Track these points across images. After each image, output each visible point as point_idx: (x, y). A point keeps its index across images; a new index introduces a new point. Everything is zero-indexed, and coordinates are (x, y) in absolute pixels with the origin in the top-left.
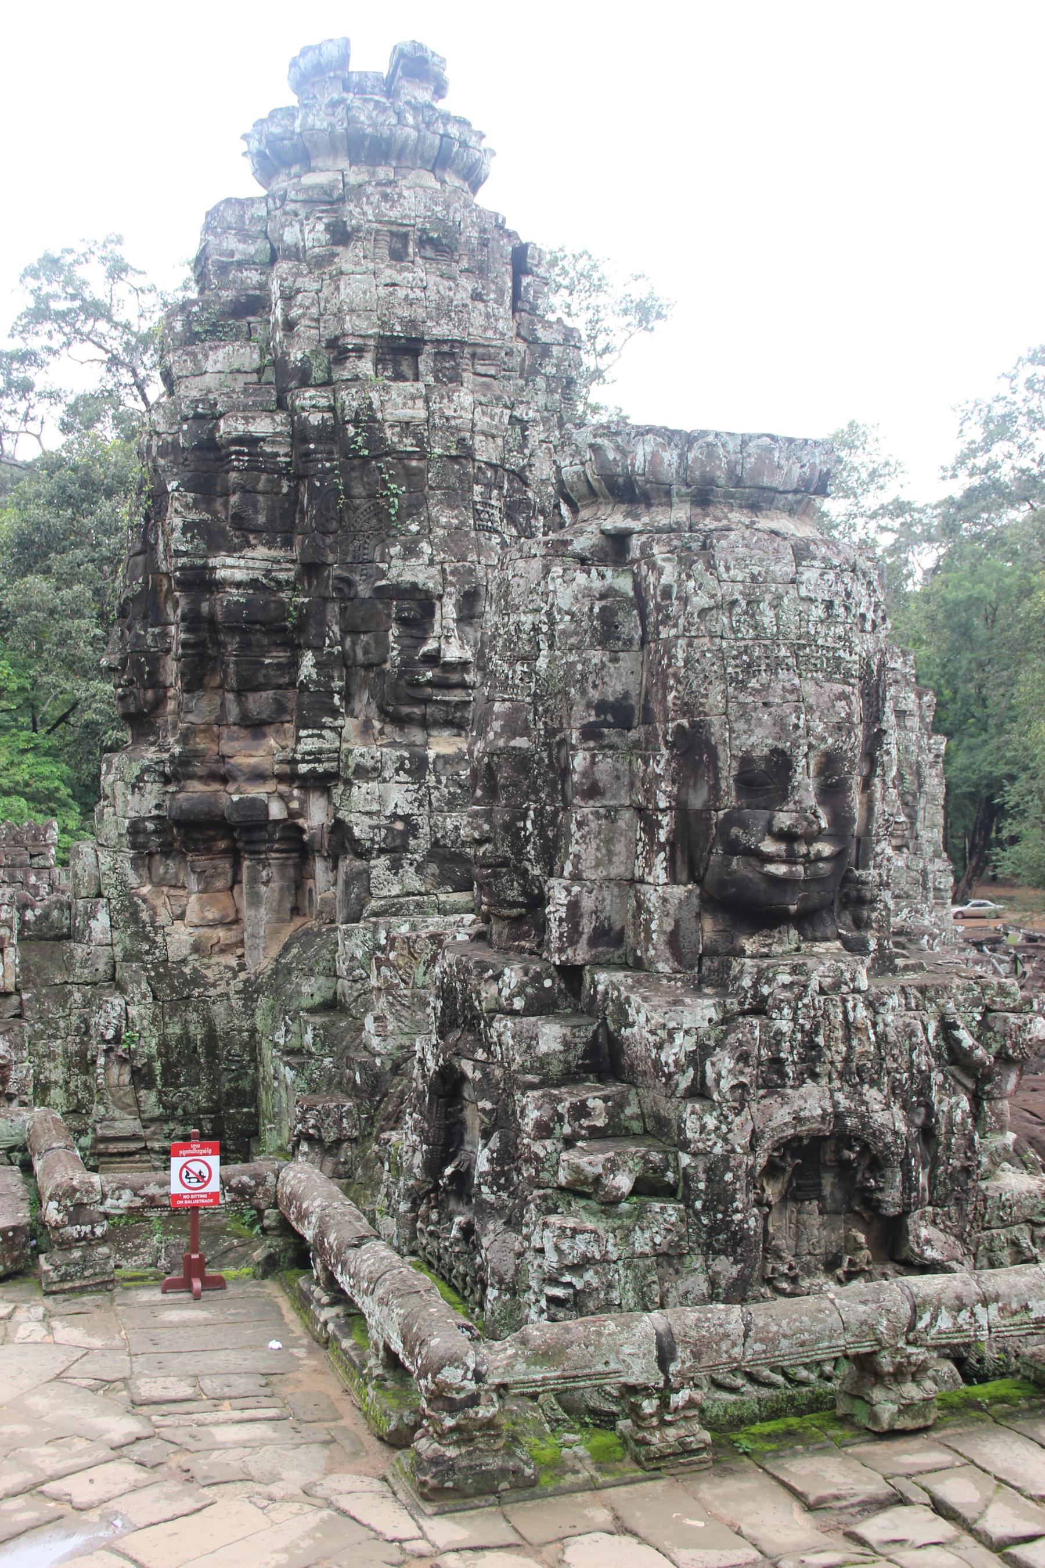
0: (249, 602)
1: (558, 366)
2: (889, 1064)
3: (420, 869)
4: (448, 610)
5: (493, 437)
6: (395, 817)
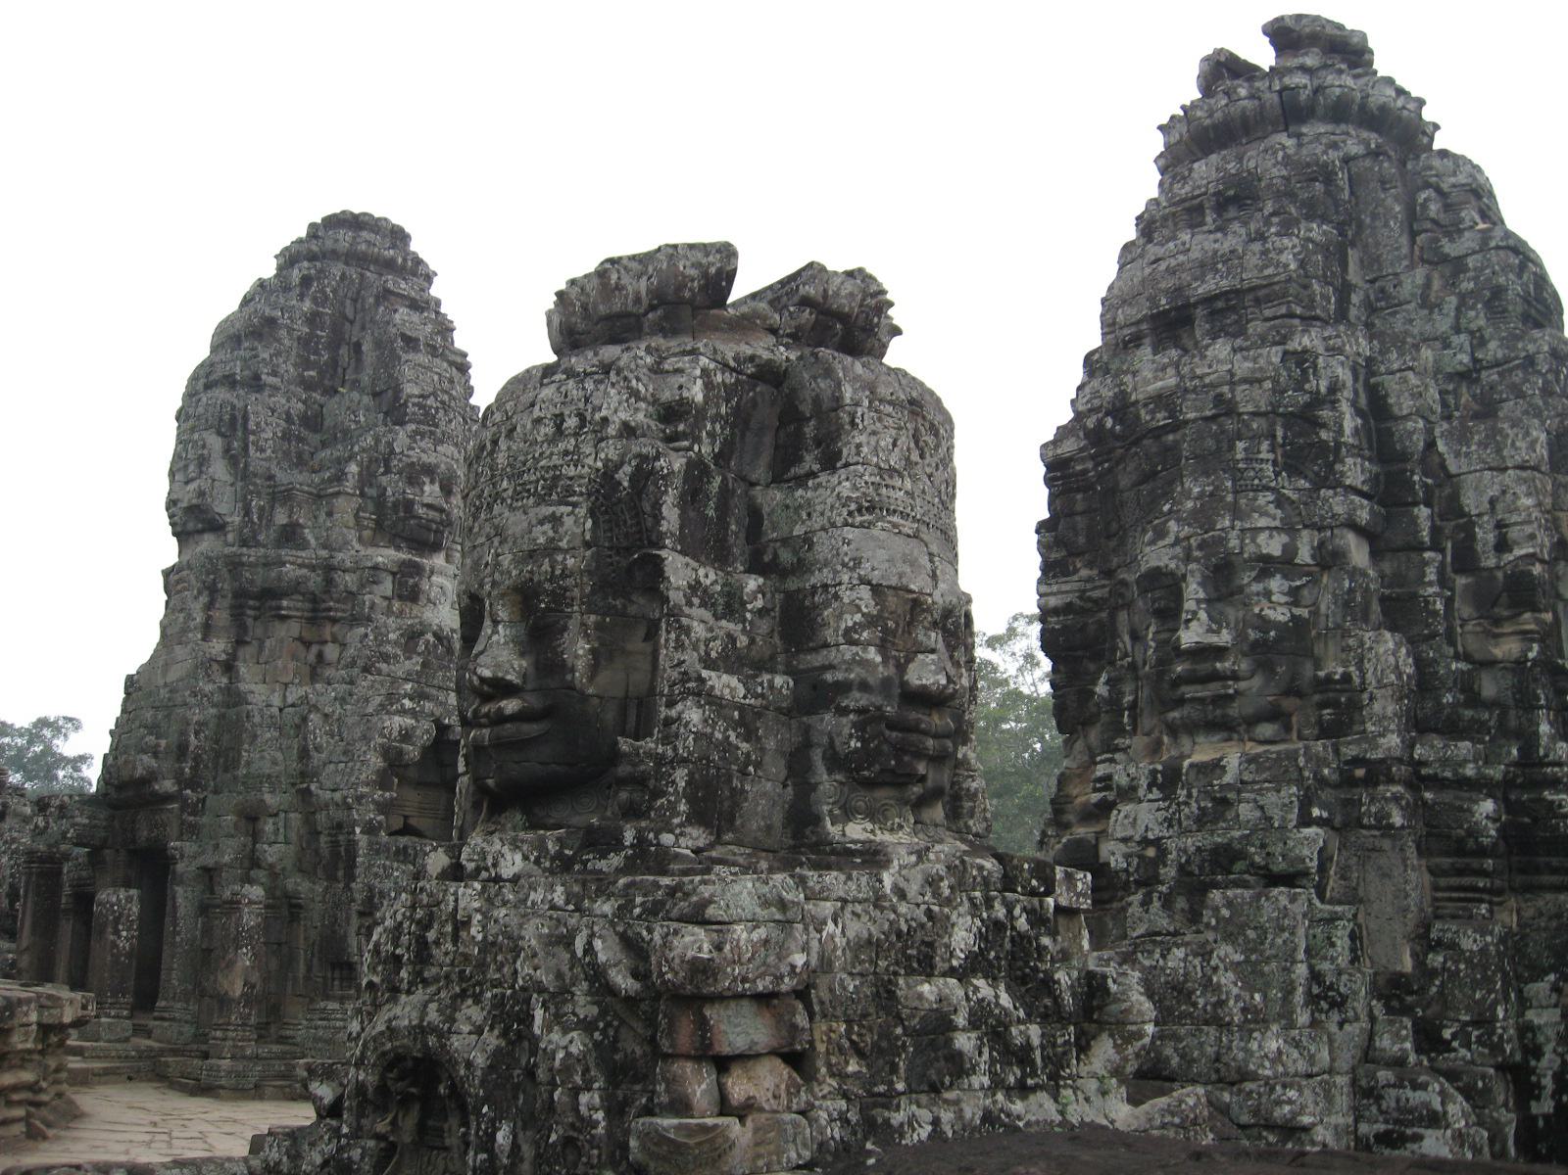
0: (1065, 627)
1: (1476, 279)
2: (493, 975)
3: (1167, 903)
4: (1193, 591)
5: (1260, 381)
6: (1145, 842)
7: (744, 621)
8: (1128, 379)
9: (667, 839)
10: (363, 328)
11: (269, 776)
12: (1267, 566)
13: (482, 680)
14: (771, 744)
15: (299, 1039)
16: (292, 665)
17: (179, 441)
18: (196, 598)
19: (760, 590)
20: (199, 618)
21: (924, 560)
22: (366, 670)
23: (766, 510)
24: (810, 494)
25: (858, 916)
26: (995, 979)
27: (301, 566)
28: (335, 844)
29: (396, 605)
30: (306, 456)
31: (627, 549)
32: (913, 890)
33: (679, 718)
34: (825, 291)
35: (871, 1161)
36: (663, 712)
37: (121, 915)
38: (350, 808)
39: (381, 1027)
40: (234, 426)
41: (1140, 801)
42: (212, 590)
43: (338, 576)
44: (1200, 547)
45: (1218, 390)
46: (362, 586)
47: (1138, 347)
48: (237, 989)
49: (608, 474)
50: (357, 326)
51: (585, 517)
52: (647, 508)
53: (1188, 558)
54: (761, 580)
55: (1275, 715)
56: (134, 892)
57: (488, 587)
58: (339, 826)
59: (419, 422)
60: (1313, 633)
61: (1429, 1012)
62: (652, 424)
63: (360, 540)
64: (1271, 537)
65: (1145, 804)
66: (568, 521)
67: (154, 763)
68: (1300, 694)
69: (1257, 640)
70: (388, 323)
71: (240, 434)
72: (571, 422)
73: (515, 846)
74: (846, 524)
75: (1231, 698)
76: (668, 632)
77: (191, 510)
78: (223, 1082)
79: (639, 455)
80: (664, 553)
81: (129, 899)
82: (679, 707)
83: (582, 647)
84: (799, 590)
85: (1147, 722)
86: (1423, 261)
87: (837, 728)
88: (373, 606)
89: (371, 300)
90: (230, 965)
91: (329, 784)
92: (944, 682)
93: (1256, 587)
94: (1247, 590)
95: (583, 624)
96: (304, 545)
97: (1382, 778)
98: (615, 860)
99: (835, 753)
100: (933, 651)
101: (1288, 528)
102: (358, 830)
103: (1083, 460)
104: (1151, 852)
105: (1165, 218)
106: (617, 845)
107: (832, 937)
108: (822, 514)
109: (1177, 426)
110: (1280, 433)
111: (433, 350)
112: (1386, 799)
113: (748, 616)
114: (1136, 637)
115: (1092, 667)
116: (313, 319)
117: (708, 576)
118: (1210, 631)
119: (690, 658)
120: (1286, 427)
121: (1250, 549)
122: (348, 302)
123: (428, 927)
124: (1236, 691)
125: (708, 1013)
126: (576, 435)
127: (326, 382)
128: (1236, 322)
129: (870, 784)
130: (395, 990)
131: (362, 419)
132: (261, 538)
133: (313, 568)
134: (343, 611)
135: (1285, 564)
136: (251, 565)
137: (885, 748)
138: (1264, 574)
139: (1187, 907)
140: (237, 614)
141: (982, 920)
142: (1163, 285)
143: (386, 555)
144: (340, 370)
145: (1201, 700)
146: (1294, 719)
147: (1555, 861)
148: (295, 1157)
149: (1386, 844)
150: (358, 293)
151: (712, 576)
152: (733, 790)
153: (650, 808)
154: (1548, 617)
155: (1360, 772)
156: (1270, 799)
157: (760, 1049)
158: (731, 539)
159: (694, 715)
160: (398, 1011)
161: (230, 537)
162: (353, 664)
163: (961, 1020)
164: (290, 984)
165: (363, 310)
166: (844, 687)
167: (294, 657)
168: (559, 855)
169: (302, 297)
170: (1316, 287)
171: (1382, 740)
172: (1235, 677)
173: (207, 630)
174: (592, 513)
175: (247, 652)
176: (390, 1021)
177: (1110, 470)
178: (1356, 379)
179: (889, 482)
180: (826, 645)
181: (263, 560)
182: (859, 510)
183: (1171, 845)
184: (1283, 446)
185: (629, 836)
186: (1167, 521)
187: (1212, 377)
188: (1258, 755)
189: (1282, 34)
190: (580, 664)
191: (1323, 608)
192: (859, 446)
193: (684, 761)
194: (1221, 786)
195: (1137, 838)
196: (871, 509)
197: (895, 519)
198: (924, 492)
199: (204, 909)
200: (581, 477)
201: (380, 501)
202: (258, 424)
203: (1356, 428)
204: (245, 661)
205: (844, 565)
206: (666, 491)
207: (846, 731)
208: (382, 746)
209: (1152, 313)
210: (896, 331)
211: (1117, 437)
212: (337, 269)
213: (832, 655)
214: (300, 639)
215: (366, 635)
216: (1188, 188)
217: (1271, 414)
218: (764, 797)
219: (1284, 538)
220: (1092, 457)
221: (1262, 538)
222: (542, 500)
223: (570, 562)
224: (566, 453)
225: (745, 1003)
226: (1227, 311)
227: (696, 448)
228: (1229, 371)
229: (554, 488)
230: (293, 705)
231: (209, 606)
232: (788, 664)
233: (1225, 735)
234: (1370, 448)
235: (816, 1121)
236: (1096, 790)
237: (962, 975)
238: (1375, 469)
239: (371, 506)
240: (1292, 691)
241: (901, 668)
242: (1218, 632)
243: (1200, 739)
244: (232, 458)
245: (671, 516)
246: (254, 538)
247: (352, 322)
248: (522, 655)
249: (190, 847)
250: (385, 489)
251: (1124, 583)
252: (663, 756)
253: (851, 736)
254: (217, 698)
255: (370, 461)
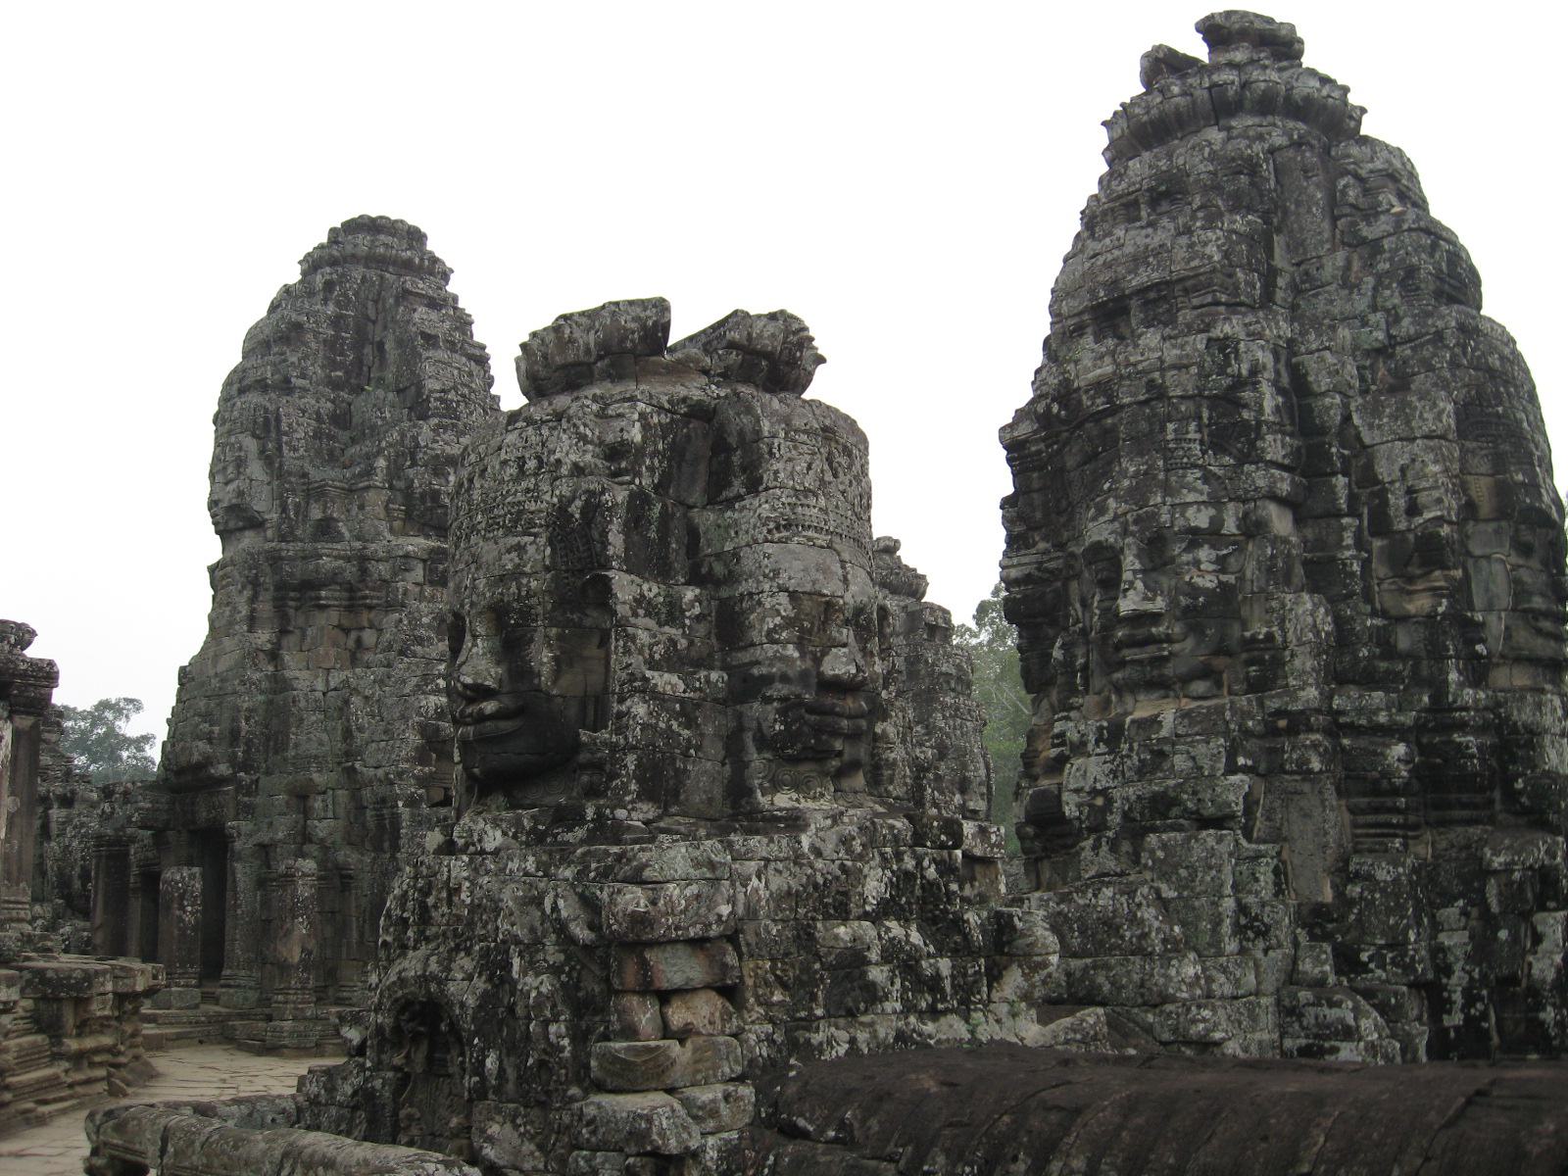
0: (1025, 597)
1: (1391, 259)
3: (1114, 847)
4: (1130, 562)
5: (1187, 367)
6: (1094, 792)
7: (683, 626)
8: (1070, 367)
9: (621, 813)
10: (385, 328)
11: (316, 757)
12: (1195, 537)
13: (466, 686)
14: (709, 730)
15: (355, 1000)
16: (333, 652)
17: (217, 444)
18: (240, 592)
19: (697, 599)
20: (244, 611)
21: (837, 568)
22: (402, 653)
23: (702, 529)
24: (736, 515)
25: (780, 872)
26: (907, 920)
27: (337, 558)
28: (380, 817)
29: (428, 590)
30: (337, 453)
31: (581, 571)
32: (828, 849)
33: (628, 712)
34: (749, 334)
35: (793, 1074)
36: (616, 707)
37: (185, 891)
38: (392, 783)
39: (393, 978)
40: (266, 428)
41: (1089, 756)
42: (255, 584)
43: (371, 566)
44: (1136, 522)
45: (1150, 376)
46: (395, 574)
47: (1081, 336)
48: (296, 956)
49: (562, 508)
50: (379, 328)
51: (545, 546)
52: (596, 536)
53: (1125, 533)
54: (697, 591)
55: (1206, 673)
56: (196, 870)
57: (467, 607)
58: (383, 800)
59: (443, 416)
60: (1240, 597)
61: (1348, 937)
62: (599, 462)
63: (391, 530)
64: (1199, 510)
65: (1093, 758)
66: (531, 549)
67: (208, 748)
68: (1229, 654)
69: (1188, 606)
70: (408, 322)
71: (273, 435)
72: (531, 464)
73: (496, 824)
74: (766, 541)
75: (1166, 659)
76: (617, 640)
77: (232, 509)
78: (286, 1042)
79: (587, 491)
80: (611, 574)
81: (192, 877)
82: (628, 703)
83: (546, 656)
84: (730, 598)
85: (1097, 682)
86: (1343, 243)
87: (764, 714)
88: (405, 593)
89: (391, 301)
90: (288, 933)
91: (371, 762)
92: (854, 671)
93: (1186, 558)
94: (1178, 561)
95: (546, 636)
96: (339, 538)
97: (1302, 728)
98: (581, 832)
99: (763, 735)
100: (845, 645)
101: (1215, 502)
102: (400, 804)
103: (1036, 441)
104: (1099, 801)
105: (1104, 213)
106: (580, 820)
107: (756, 890)
108: (747, 532)
109: (1114, 410)
110: (1205, 414)
111: (452, 346)
112: (1305, 746)
113: (687, 622)
114: (1085, 604)
115: (1051, 632)
116: (337, 322)
117: (652, 590)
118: (1146, 598)
119: (636, 661)
120: (1211, 409)
121: (1180, 523)
122: (370, 303)
123: (428, 894)
124: (1170, 653)
125: (648, 956)
126: (536, 475)
127: (353, 381)
128: (1168, 311)
129: (794, 760)
130: (404, 947)
131: (388, 415)
132: (298, 532)
133: (348, 559)
134: (378, 598)
135: (1212, 535)
136: (292, 559)
137: (806, 729)
138: (1193, 545)
139: (1131, 850)
140: (280, 605)
141: (893, 872)
142: (1101, 279)
143: (416, 544)
144: (365, 369)
145: (1140, 662)
146: (1225, 676)
147: (1465, 797)
148: (331, 1090)
149: (1306, 787)
150: (379, 294)
151: (655, 590)
152: (677, 770)
153: (608, 788)
154: (1458, 573)
155: (1282, 723)
156: (1201, 750)
157: (695, 984)
158: (672, 556)
159: (640, 709)
160: (406, 964)
161: (269, 533)
162: (389, 648)
163: (874, 955)
164: (344, 949)
165: (384, 310)
166: (768, 680)
167: (335, 644)
168: (534, 830)
169: (325, 301)
170: (1240, 275)
171: (1302, 693)
172: (1169, 639)
173: (252, 621)
174: (550, 542)
175: (291, 640)
176: (400, 972)
177: (1060, 450)
178: (1277, 359)
179: (804, 501)
180: (753, 645)
181: (300, 554)
182: (777, 528)
183: (1116, 794)
184: (1209, 426)
185: (590, 813)
186: (1106, 499)
187: (1145, 364)
188: (1192, 710)
189: (1214, 30)
190: (545, 670)
191: (1248, 574)
192: (776, 472)
193: (634, 748)
194: (1158, 739)
195: (1087, 789)
196: (787, 527)
197: (810, 533)
198: (837, 507)
199: (261, 883)
200: (541, 511)
201: (408, 493)
202: (290, 425)
203: (1277, 406)
204: (289, 649)
205: (765, 576)
206: (611, 521)
207: (771, 717)
208: (420, 724)
209: (1095, 305)
210: (821, 360)
211: (1063, 422)
212: (357, 273)
213: (757, 653)
214: (339, 626)
215: (401, 621)
216: (1124, 185)
217: (1197, 397)
218: (704, 774)
219: (1212, 512)
220: (1043, 440)
221: (1190, 512)
222: (509, 531)
223: (534, 584)
224: (528, 490)
225: (679, 946)
226: (1159, 301)
227: (637, 481)
228: (1159, 358)
229: (520, 521)
230: (335, 689)
231: (253, 599)
232: (724, 661)
233: (1162, 692)
234: (1292, 424)
235: (747, 1041)
236: (1054, 746)
237: (876, 918)
238: (1296, 443)
239: (399, 497)
240: (1221, 650)
241: (818, 661)
242: (1152, 600)
243: (1141, 697)
244: (267, 459)
245: (616, 541)
246: (292, 533)
247: (374, 322)
248: (498, 663)
249: (246, 826)
250: (412, 481)
251: (1073, 555)
252: (617, 744)
253: (775, 720)
254: (264, 685)
255: (397, 456)
